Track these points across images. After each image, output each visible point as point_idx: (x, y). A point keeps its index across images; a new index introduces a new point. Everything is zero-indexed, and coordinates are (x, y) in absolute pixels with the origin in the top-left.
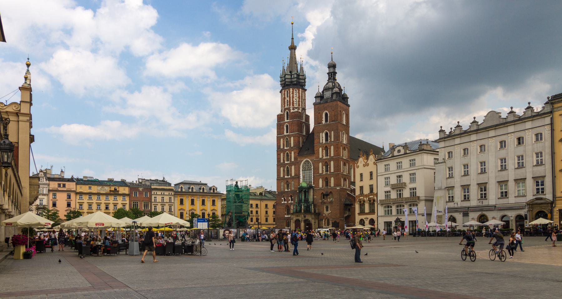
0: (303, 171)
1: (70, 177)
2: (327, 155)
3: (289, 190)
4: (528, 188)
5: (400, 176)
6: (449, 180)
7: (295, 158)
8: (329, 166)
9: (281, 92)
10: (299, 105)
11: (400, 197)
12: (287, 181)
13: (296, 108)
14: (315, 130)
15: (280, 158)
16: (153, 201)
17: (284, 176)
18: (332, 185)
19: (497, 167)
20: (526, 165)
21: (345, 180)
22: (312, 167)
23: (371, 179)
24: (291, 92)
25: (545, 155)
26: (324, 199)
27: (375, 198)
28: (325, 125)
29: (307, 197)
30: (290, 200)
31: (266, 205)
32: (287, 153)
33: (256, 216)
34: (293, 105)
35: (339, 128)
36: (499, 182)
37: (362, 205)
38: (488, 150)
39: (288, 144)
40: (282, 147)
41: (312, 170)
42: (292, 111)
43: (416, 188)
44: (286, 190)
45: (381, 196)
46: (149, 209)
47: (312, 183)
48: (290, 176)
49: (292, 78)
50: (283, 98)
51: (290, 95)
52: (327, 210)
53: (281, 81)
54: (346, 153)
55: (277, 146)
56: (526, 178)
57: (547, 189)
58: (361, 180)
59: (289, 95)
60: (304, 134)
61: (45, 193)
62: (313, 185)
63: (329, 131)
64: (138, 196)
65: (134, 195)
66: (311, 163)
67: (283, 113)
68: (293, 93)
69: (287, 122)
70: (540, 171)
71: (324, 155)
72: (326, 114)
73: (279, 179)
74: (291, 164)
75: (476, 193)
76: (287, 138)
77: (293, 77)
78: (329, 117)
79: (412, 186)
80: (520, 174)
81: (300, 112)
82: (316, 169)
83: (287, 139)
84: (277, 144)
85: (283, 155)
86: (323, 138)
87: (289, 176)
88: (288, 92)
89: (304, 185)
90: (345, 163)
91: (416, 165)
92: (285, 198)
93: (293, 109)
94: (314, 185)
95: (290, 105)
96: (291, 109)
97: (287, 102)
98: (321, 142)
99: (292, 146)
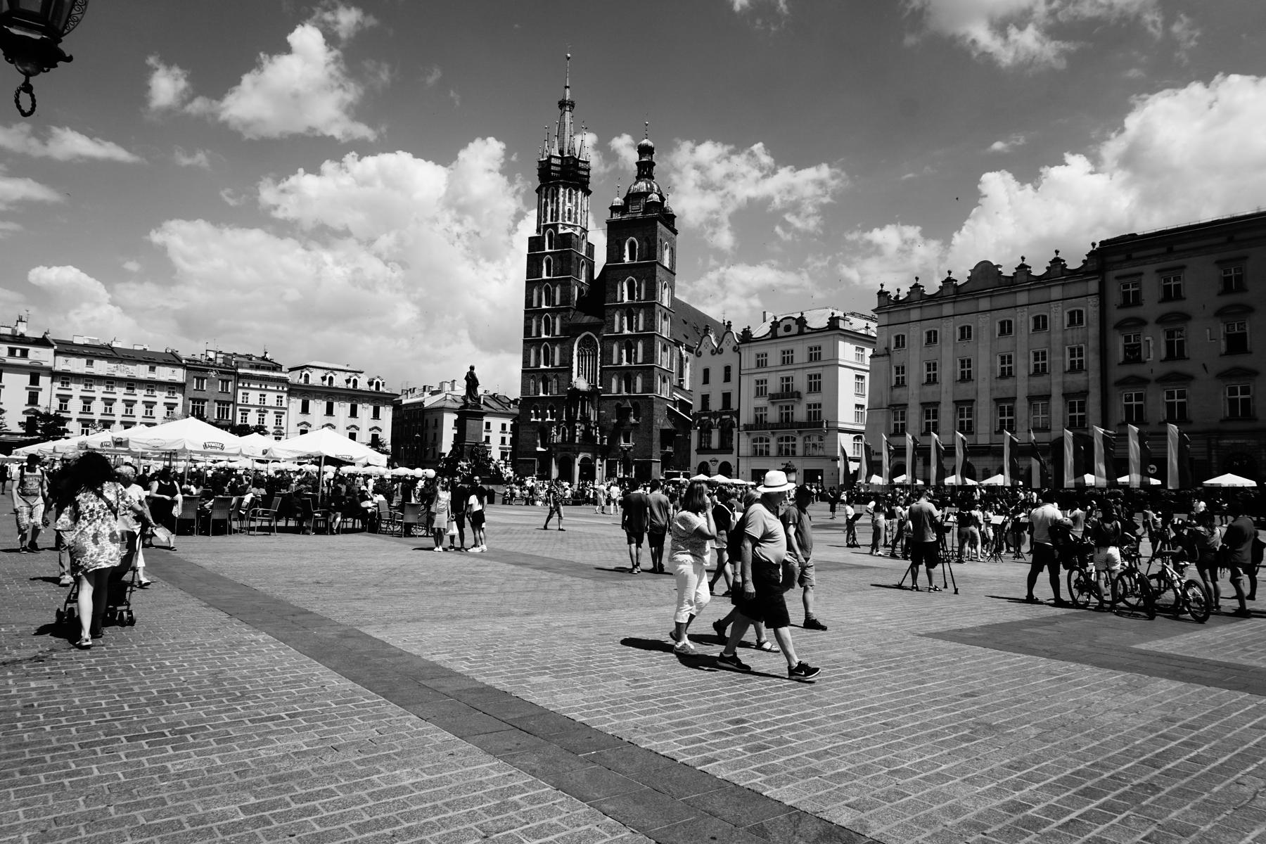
0: (578, 356)
1: (40, 336)
4: (1053, 415)
5: (788, 379)
6: (897, 391)
9: (538, 191)
10: (576, 222)
11: (787, 419)
13: (570, 226)
16: (239, 401)
18: (639, 389)
19: (992, 370)
20: (1050, 370)
21: (664, 381)
23: (727, 378)
25: (1087, 353)
27: (735, 419)
31: (488, 425)
32: (547, 319)
35: (658, 274)
36: (998, 401)
37: (705, 431)
38: (977, 337)
43: (820, 405)
44: (541, 394)
45: (746, 417)
46: (230, 418)
51: (558, 199)
52: (627, 441)
56: (1050, 396)
57: (1090, 418)
58: (706, 381)
60: (583, 280)
70: (1078, 380)
71: (626, 326)
72: (632, 245)
73: (527, 372)
74: (553, 342)
75: (951, 420)
79: (813, 398)
80: (1039, 383)
81: (577, 236)
82: (607, 355)
83: (547, 287)
86: (622, 291)
89: (582, 384)
91: (823, 358)
93: (564, 229)
95: (557, 219)
98: (619, 299)
99: (557, 303)
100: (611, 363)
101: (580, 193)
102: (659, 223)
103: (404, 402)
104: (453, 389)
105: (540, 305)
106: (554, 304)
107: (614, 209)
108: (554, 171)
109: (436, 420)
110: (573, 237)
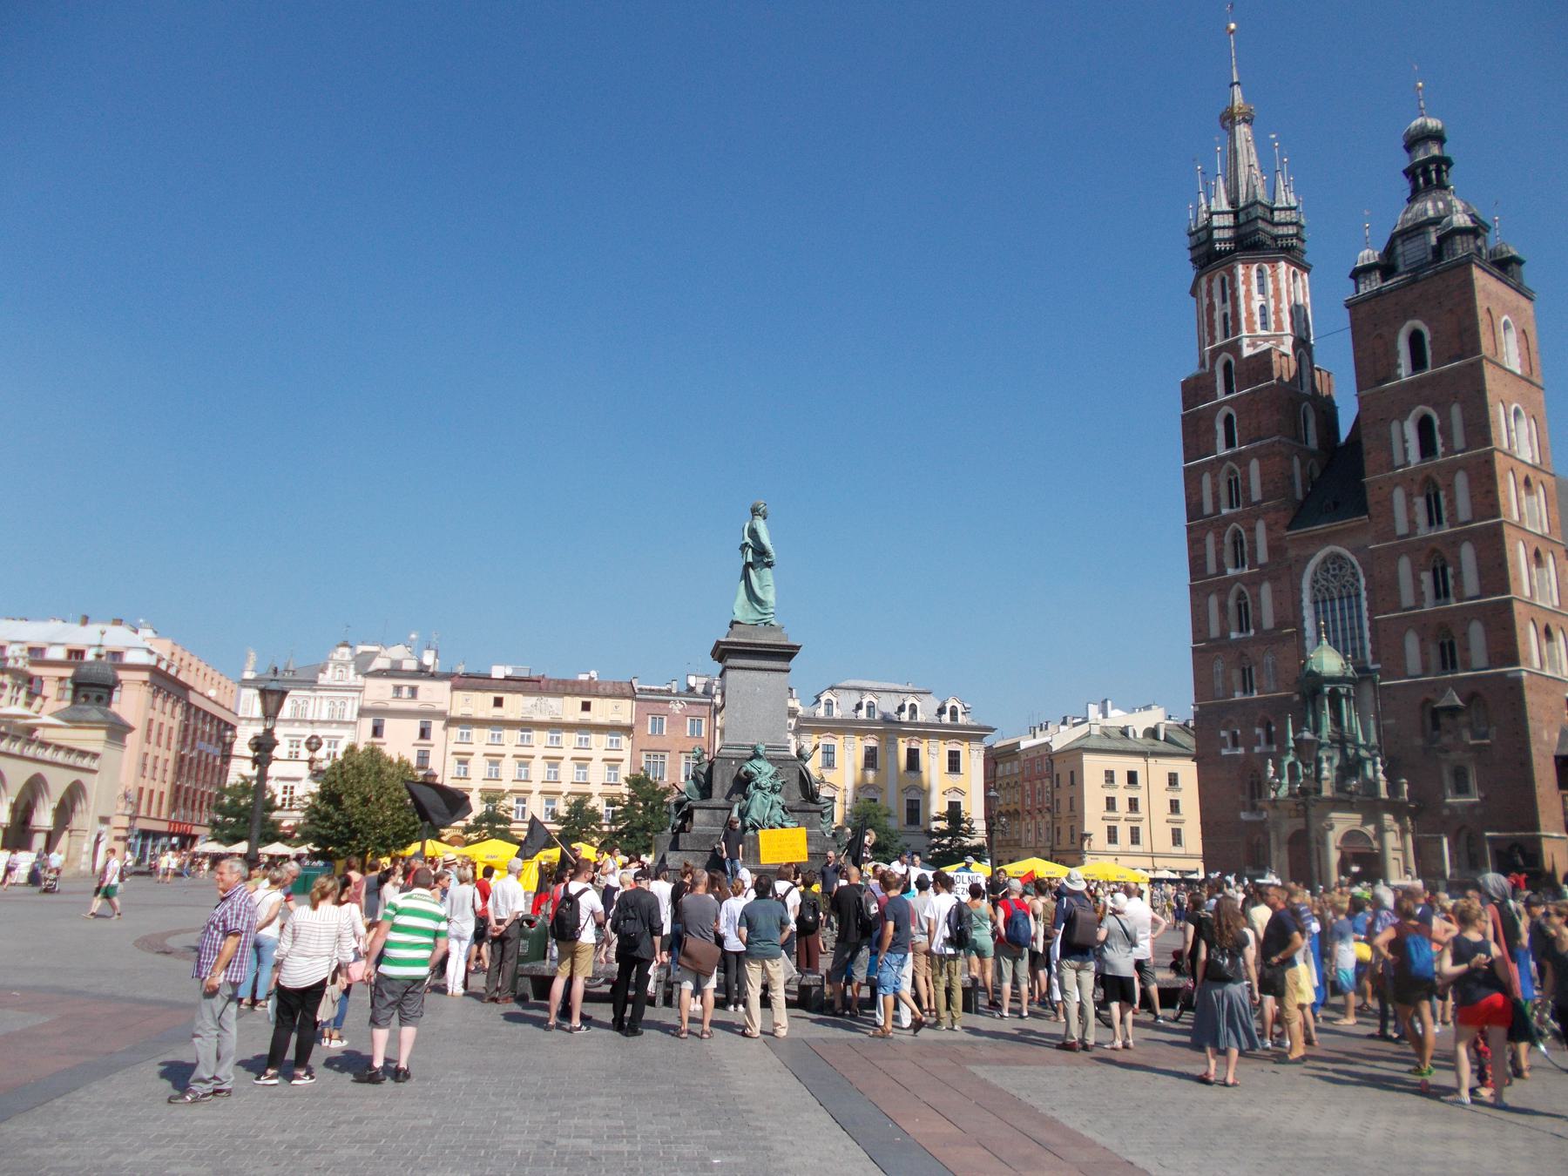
0: (1316, 603)
2: (1434, 517)
3: (1255, 695)
7: (1274, 549)
8: (1450, 571)
9: (1194, 292)
10: (1279, 326)
12: (1242, 654)
13: (1266, 339)
14: (1362, 423)
15: (1205, 555)
17: (1224, 634)
21: (1548, 633)
22: (1363, 581)
24: (1241, 278)
26: (1436, 733)
28: (1411, 383)
29: (1346, 724)
30: (1263, 738)
32: (1237, 534)
33: (1118, 819)
34: (1251, 329)
39: (1237, 490)
40: (1208, 508)
41: (1364, 594)
42: (1247, 352)
44: (1238, 696)
47: (1369, 657)
48: (1252, 632)
49: (1241, 221)
50: (1205, 307)
51: (1234, 291)
53: (1191, 249)
54: (1539, 506)
55: (1187, 505)
59: (1228, 292)
60: (1313, 443)
61: (347, 718)
62: (1373, 663)
63: (1435, 406)
64: (664, 733)
65: (650, 728)
66: (1356, 563)
67: (1208, 366)
68: (1247, 282)
69: (1225, 403)
71: (1422, 519)
72: (1416, 339)
76: (1230, 467)
77: (1242, 217)
78: (1431, 342)
82: (1384, 591)
84: (1188, 498)
85: (1217, 543)
86: (1405, 441)
87: (1248, 629)
88: (1227, 278)
90: (1537, 554)
92: (1234, 735)
93: (1254, 345)
94: (1378, 666)
95: (1237, 330)
96: (1244, 346)
97: (1226, 323)
98: (1398, 459)
99: (1256, 495)
100: (1397, 607)
101: (1283, 265)
102: (1477, 273)
103: (1023, 745)
104: (1105, 716)
105: (1217, 509)
106: (1248, 502)
107: (1358, 274)
108: (1220, 241)
109: (1072, 773)
110: (1275, 357)
